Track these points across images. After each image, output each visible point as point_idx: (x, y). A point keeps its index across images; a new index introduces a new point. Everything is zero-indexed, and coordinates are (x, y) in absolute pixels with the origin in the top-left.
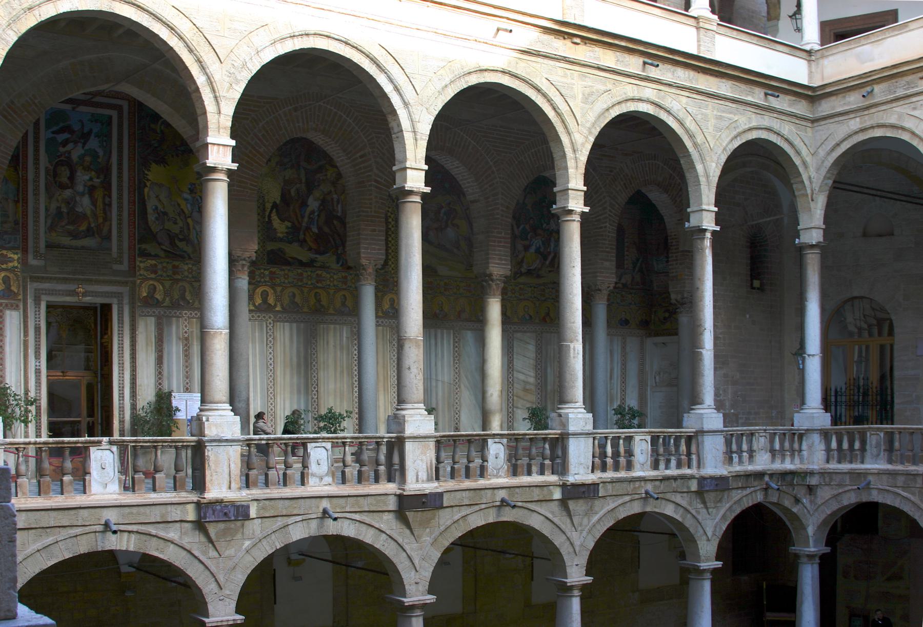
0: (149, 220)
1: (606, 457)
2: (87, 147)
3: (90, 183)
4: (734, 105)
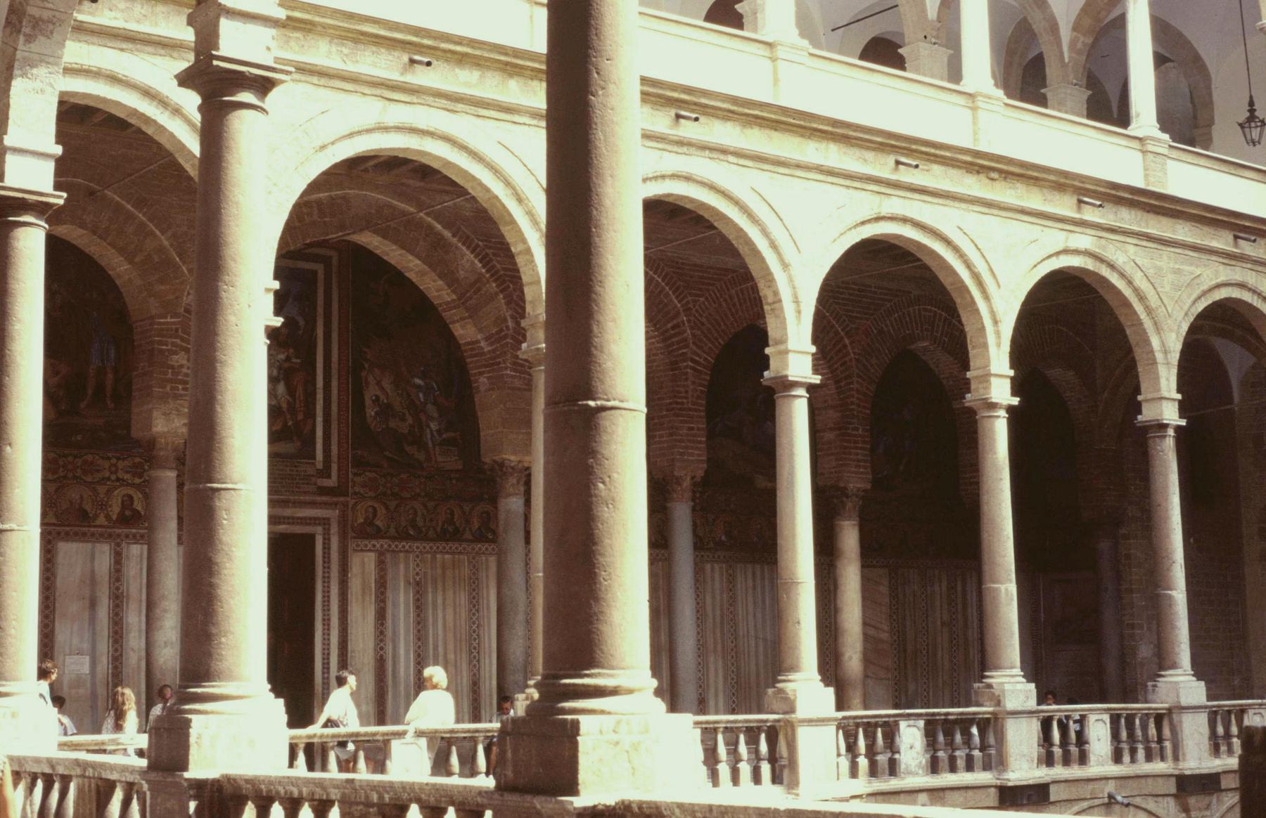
0: (368, 415)
1: (1051, 745)
3: (286, 365)
4: (1195, 254)
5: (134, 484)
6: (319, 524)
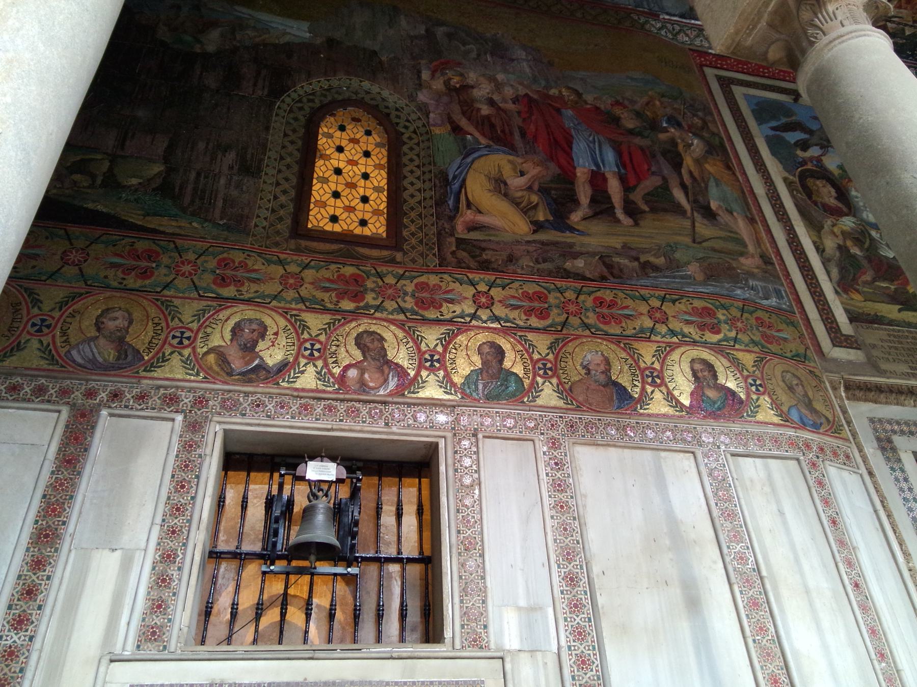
5: (706, 343)
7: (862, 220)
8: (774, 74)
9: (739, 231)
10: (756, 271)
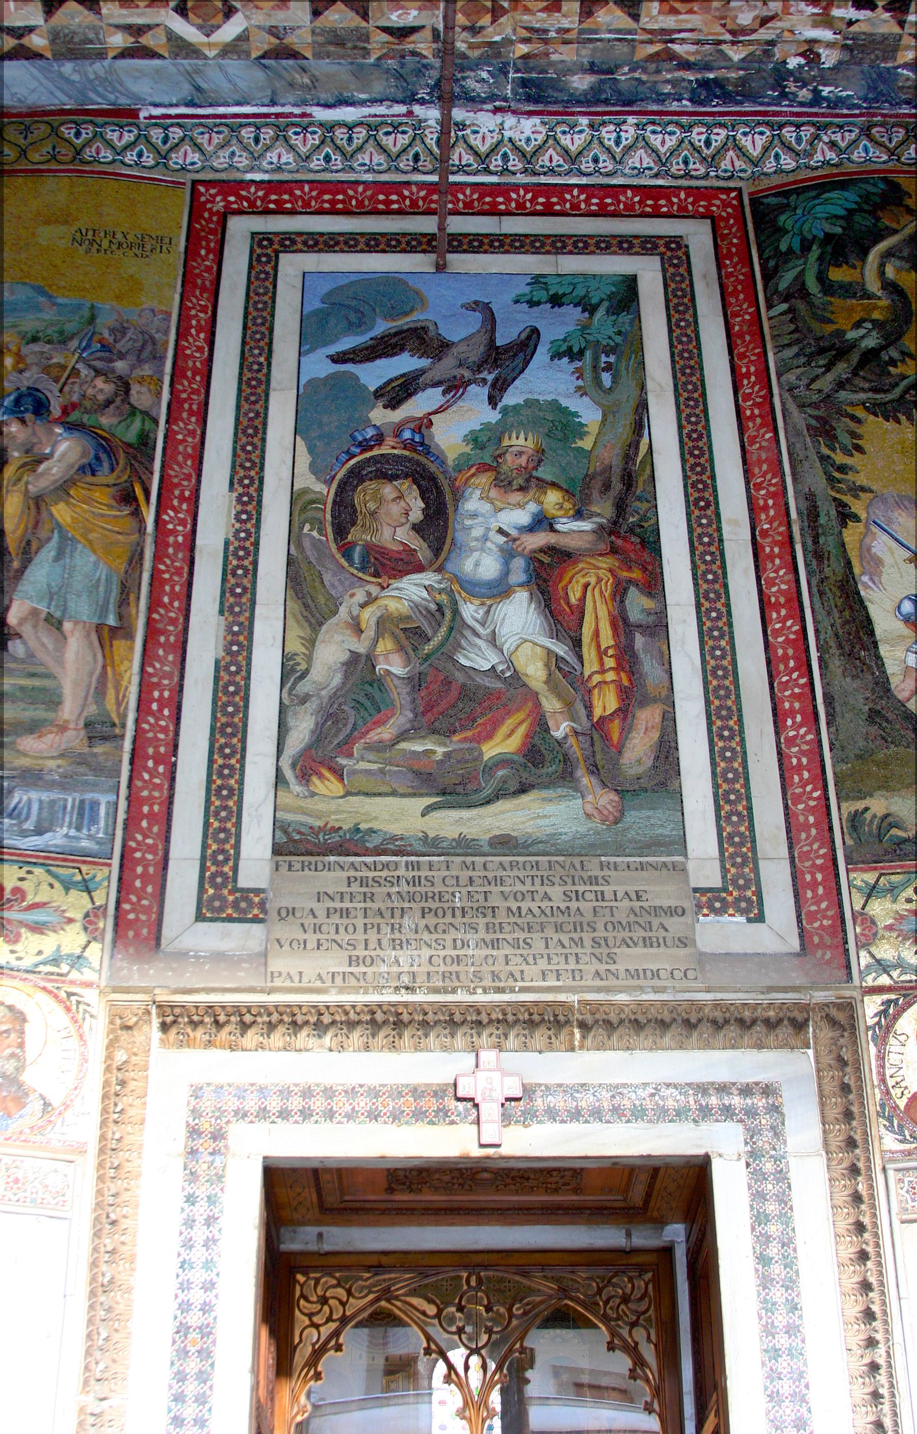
2: (511, 398)
3: (540, 539)
6: (728, 1112)
7: (457, 579)
8: (414, 203)
9: (55, 669)
10: (52, 764)
